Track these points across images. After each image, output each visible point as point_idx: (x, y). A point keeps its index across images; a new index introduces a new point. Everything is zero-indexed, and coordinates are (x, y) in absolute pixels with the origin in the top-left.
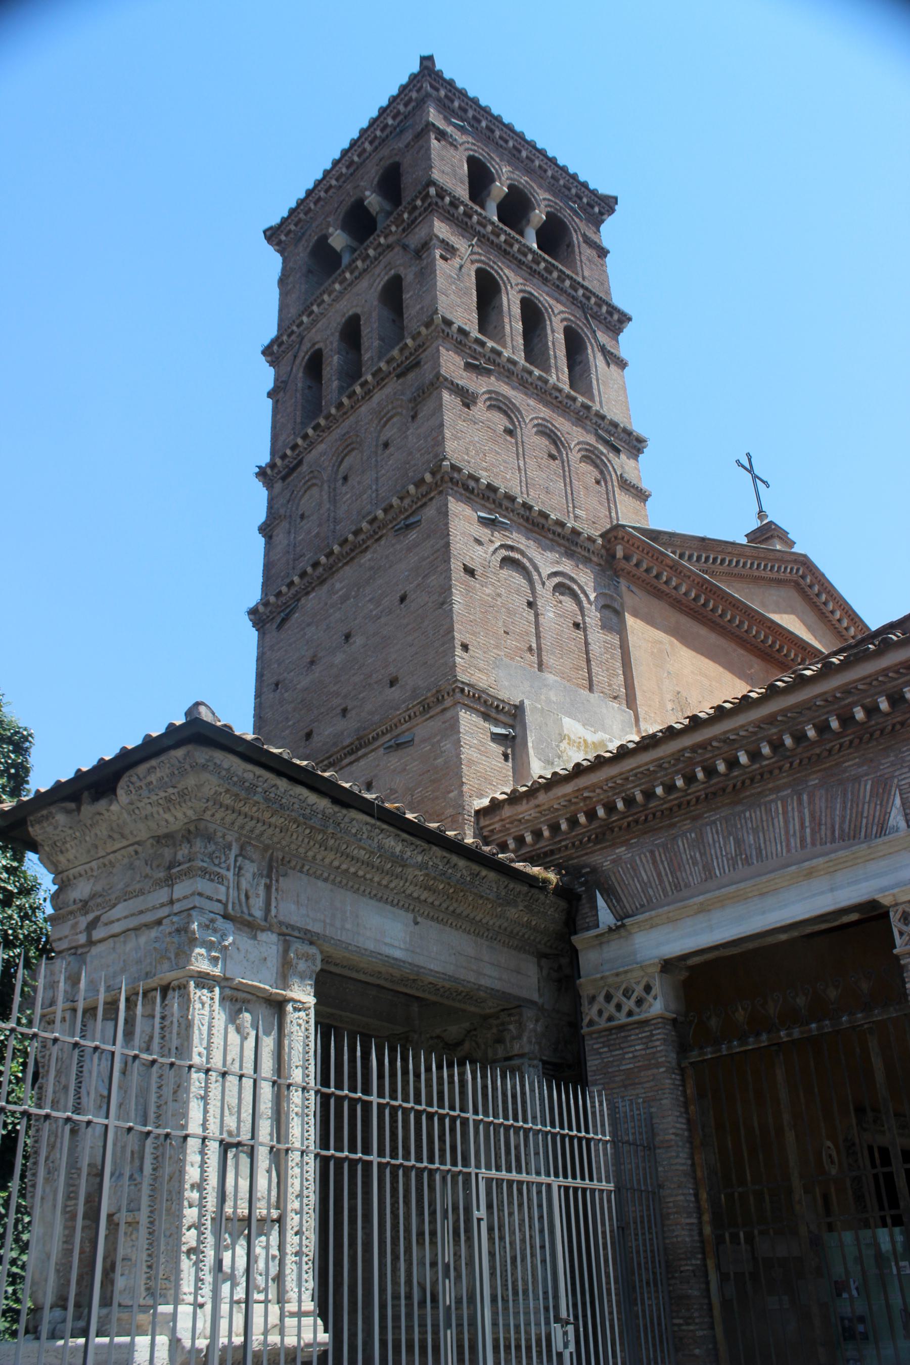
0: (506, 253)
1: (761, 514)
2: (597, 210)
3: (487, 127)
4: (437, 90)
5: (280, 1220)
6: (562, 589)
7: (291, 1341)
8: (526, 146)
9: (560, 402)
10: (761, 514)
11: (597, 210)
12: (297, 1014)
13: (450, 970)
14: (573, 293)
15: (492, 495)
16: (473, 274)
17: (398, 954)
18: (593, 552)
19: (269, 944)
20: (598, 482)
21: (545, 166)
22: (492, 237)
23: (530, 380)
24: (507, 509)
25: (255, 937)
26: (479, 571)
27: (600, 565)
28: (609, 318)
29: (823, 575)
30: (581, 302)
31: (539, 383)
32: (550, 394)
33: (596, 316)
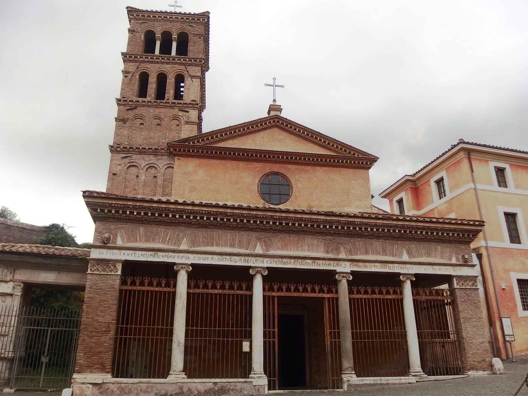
0: (152, 62)
1: (274, 101)
2: (201, 20)
3: (153, 16)
4: (133, 15)
5: (8, 335)
6: (151, 168)
7: (6, 356)
8: (169, 14)
9: (164, 106)
10: (274, 101)
11: (201, 20)
12: (16, 297)
13: (69, 282)
14: (180, 62)
15: (126, 150)
16: (138, 77)
17: (51, 281)
18: (164, 152)
19: (11, 284)
20: (178, 125)
21: (177, 17)
22: (145, 60)
23: (151, 104)
24: (131, 151)
25: (7, 284)
26: (118, 173)
27: (167, 155)
28: (195, 63)
29: (286, 119)
30: (183, 63)
31: (155, 104)
32: (159, 105)
33: (190, 65)
